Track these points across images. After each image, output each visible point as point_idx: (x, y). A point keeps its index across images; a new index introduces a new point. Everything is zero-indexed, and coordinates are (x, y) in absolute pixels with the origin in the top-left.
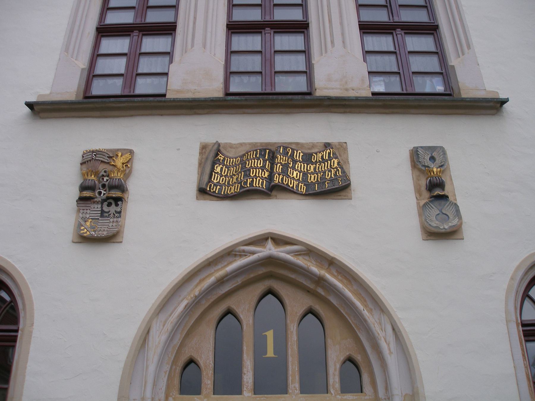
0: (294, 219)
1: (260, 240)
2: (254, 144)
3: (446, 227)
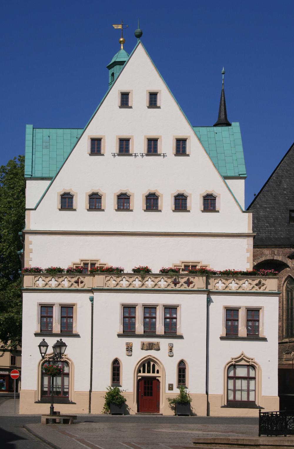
0: (152, 353)
1: (148, 356)
2: (148, 342)
3: (171, 355)
